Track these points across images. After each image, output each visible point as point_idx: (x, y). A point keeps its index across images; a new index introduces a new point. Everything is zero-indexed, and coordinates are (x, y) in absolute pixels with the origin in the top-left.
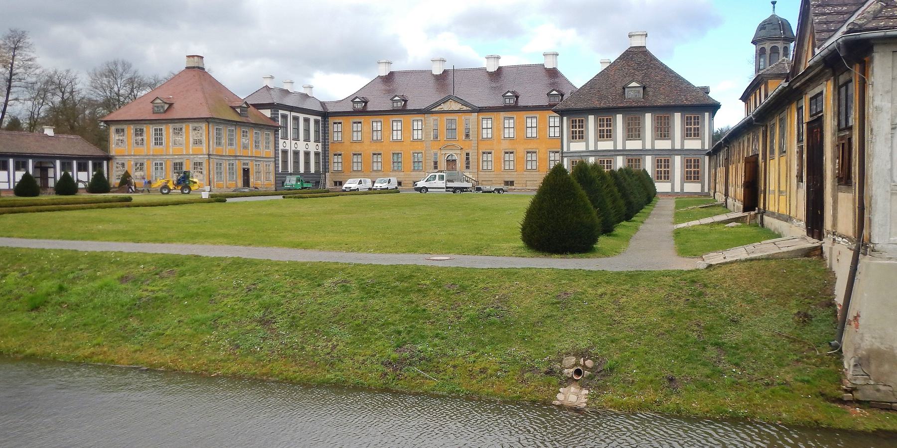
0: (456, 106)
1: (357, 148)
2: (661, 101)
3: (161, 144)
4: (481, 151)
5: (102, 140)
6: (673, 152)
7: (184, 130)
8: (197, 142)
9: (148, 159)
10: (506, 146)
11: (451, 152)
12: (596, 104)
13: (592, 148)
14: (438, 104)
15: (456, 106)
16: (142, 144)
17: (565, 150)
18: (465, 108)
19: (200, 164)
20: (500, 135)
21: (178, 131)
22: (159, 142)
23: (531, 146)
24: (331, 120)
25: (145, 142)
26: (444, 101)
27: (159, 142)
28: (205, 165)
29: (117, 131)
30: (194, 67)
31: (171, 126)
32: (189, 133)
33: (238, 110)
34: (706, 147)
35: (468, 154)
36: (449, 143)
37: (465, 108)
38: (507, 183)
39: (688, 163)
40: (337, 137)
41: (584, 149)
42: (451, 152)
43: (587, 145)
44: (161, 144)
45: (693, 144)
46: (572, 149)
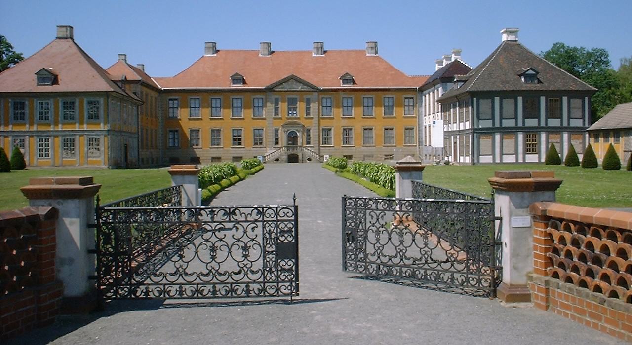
7: (77, 104)
12: (501, 87)
13: (497, 125)
33: (120, 84)
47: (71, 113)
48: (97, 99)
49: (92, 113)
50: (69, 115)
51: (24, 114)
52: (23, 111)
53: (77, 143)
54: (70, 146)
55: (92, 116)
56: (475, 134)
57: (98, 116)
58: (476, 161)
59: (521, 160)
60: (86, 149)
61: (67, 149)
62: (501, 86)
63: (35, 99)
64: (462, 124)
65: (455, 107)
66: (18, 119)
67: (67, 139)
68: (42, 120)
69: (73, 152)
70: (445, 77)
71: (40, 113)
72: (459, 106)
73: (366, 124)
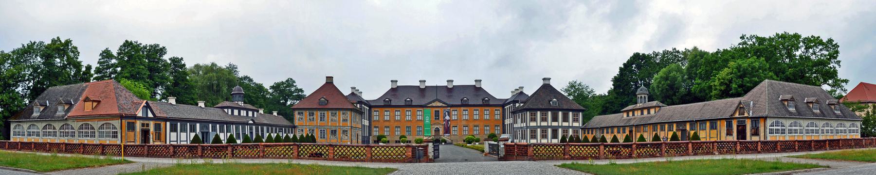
0: (440, 104)
1: (387, 124)
2: (565, 107)
5: (290, 118)
6: (548, 127)
8: (345, 120)
10: (464, 123)
12: (541, 107)
14: (431, 103)
15: (440, 104)
21: (334, 115)
24: (373, 110)
26: (434, 101)
28: (349, 132)
29: (299, 114)
31: (330, 113)
32: (341, 116)
39: (542, 131)
40: (376, 118)
45: (576, 124)
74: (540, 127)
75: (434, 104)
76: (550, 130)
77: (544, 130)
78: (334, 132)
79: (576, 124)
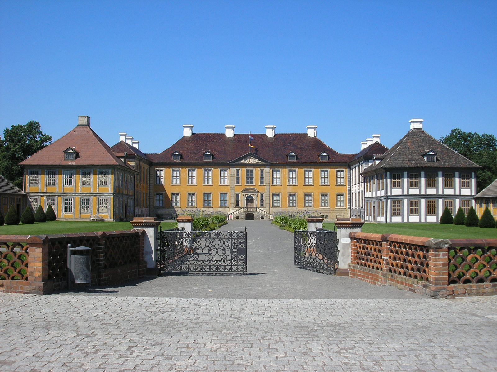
3: (71, 184)
4: (271, 194)
6: (420, 196)
9: (59, 196)
11: (250, 194)
13: (405, 193)
14: (241, 159)
16: (54, 184)
17: (389, 194)
18: (261, 162)
19: (106, 200)
20: (286, 182)
22: (68, 182)
23: (308, 191)
25: (56, 183)
27: (68, 182)
30: (85, 125)
34: (473, 194)
35: (262, 195)
36: (248, 187)
37: (261, 162)
38: (322, 216)
39: (411, 204)
41: (400, 194)
42: (250, 194)
43: (403, 191)
44: (71, 184)
46: (393, 194)
47: (88, 180)
48: (107, 170)
49: (102, 180)
50: (86, 182)
51: (54, 180)
52: (54, 179)
53: (91, 202)
54: (87, 204)
55: (103, 183)
56: (389, 201)
57: (107, 183)
58: (388, 220)
59: (423, 220)
60: (97, 207)
61: (85, 207)
62: (408, 163)
63: (63, 170)
64: (379, 192)
65: (374, 179)
66: (50, 184)
67: (85, 199)
68: (67, 185)
69: (88, 209)
70: (367, 155)
71: (66, 179)
72: (377, 178)
73: (307, 191)
74: (408, 196)
75: (246, 162)
76: (423, 201)
77: (414, 200)
78: (86, 203)
79: (466, 192)
